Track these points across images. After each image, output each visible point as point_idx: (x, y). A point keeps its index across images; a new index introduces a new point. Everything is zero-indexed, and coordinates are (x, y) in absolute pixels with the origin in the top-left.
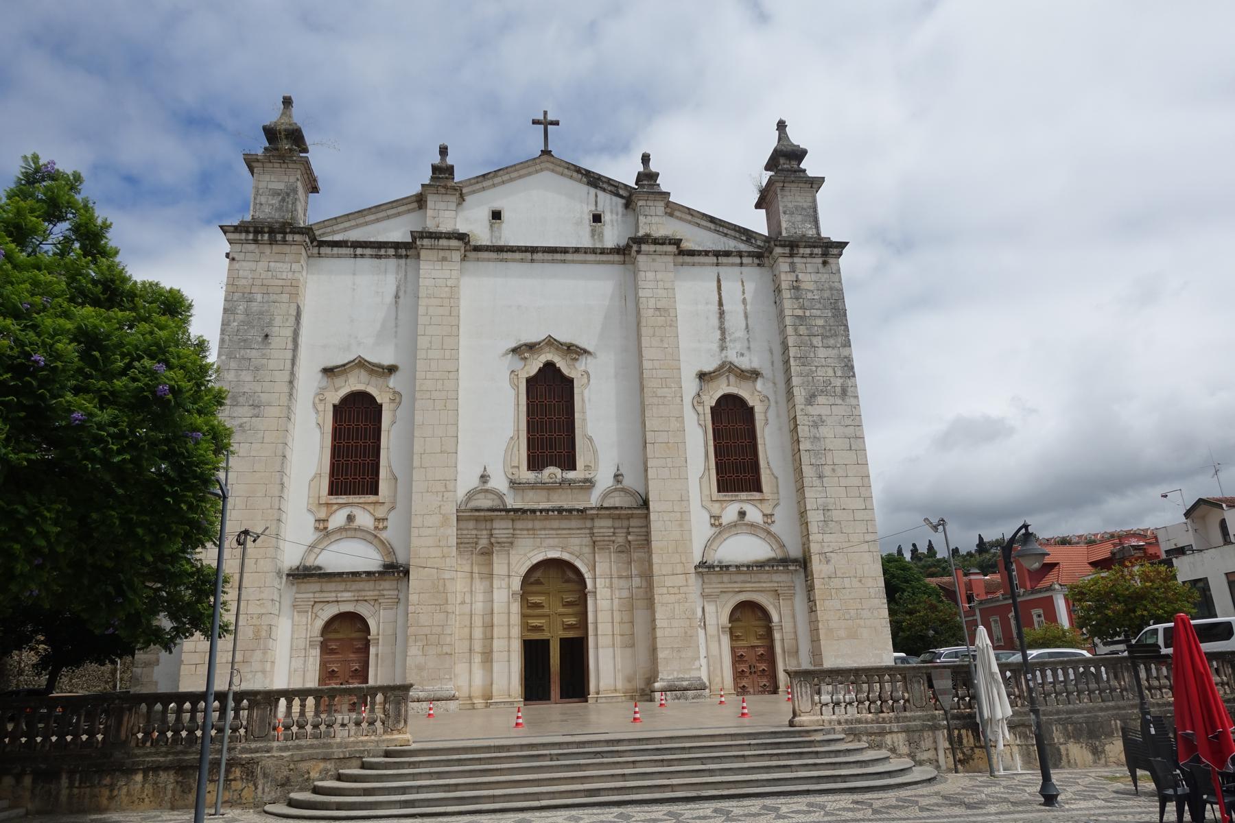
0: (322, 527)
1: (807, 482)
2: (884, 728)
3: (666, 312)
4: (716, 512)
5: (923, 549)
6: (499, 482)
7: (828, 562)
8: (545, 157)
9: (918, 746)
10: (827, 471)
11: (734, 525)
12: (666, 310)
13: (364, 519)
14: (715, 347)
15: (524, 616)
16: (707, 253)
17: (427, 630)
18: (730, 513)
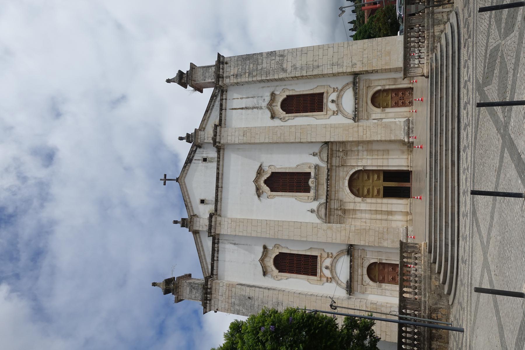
0: (329, 280)
1: (320, 73)
2: (432, 36)
3: (245, 132)
4: (331, 113)
5: (352, 26)
6: (314, 205)
7: (356, 64)
8: (179, 180)
9: (441, 21)
10: (316, 64)
11: (338, 105)
12: (244, 132)
13: (328, 262)
14: (260, 111)
15: (373, 197)
16: (221, 114)
17: (377, 238)
18: (332, 107)
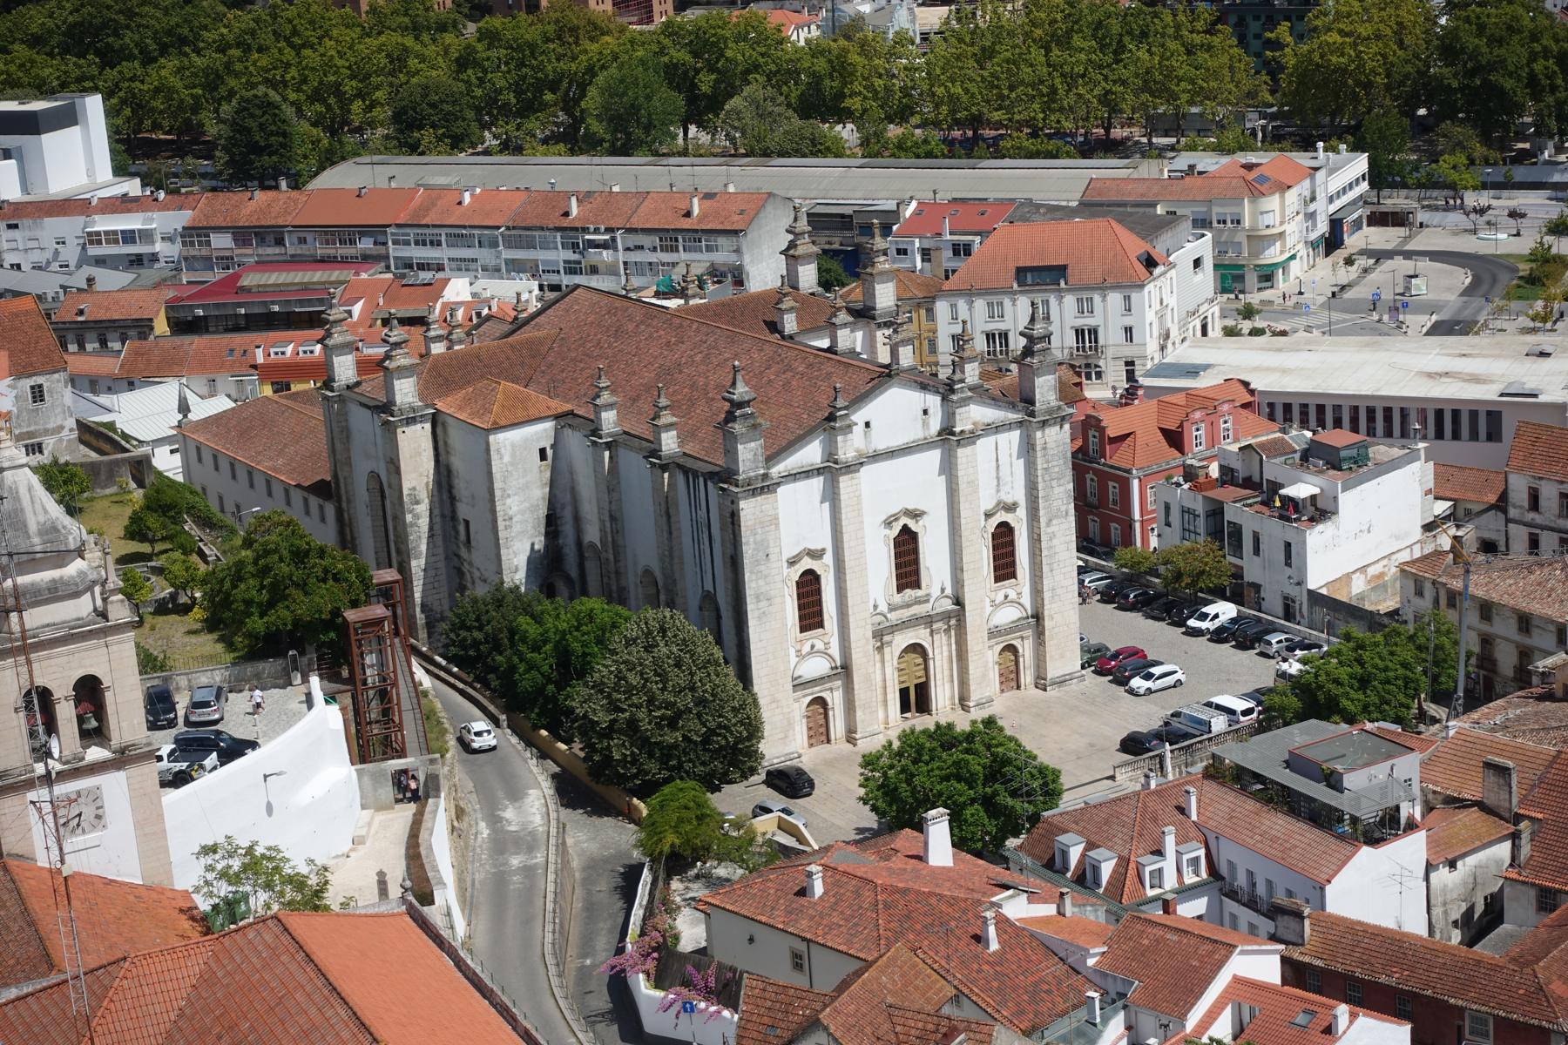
6: (883, 608)
14: (994, 491)
